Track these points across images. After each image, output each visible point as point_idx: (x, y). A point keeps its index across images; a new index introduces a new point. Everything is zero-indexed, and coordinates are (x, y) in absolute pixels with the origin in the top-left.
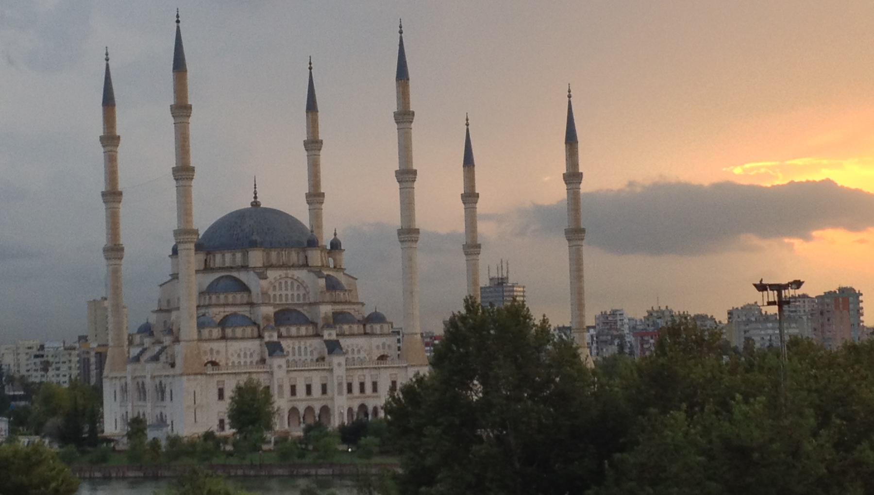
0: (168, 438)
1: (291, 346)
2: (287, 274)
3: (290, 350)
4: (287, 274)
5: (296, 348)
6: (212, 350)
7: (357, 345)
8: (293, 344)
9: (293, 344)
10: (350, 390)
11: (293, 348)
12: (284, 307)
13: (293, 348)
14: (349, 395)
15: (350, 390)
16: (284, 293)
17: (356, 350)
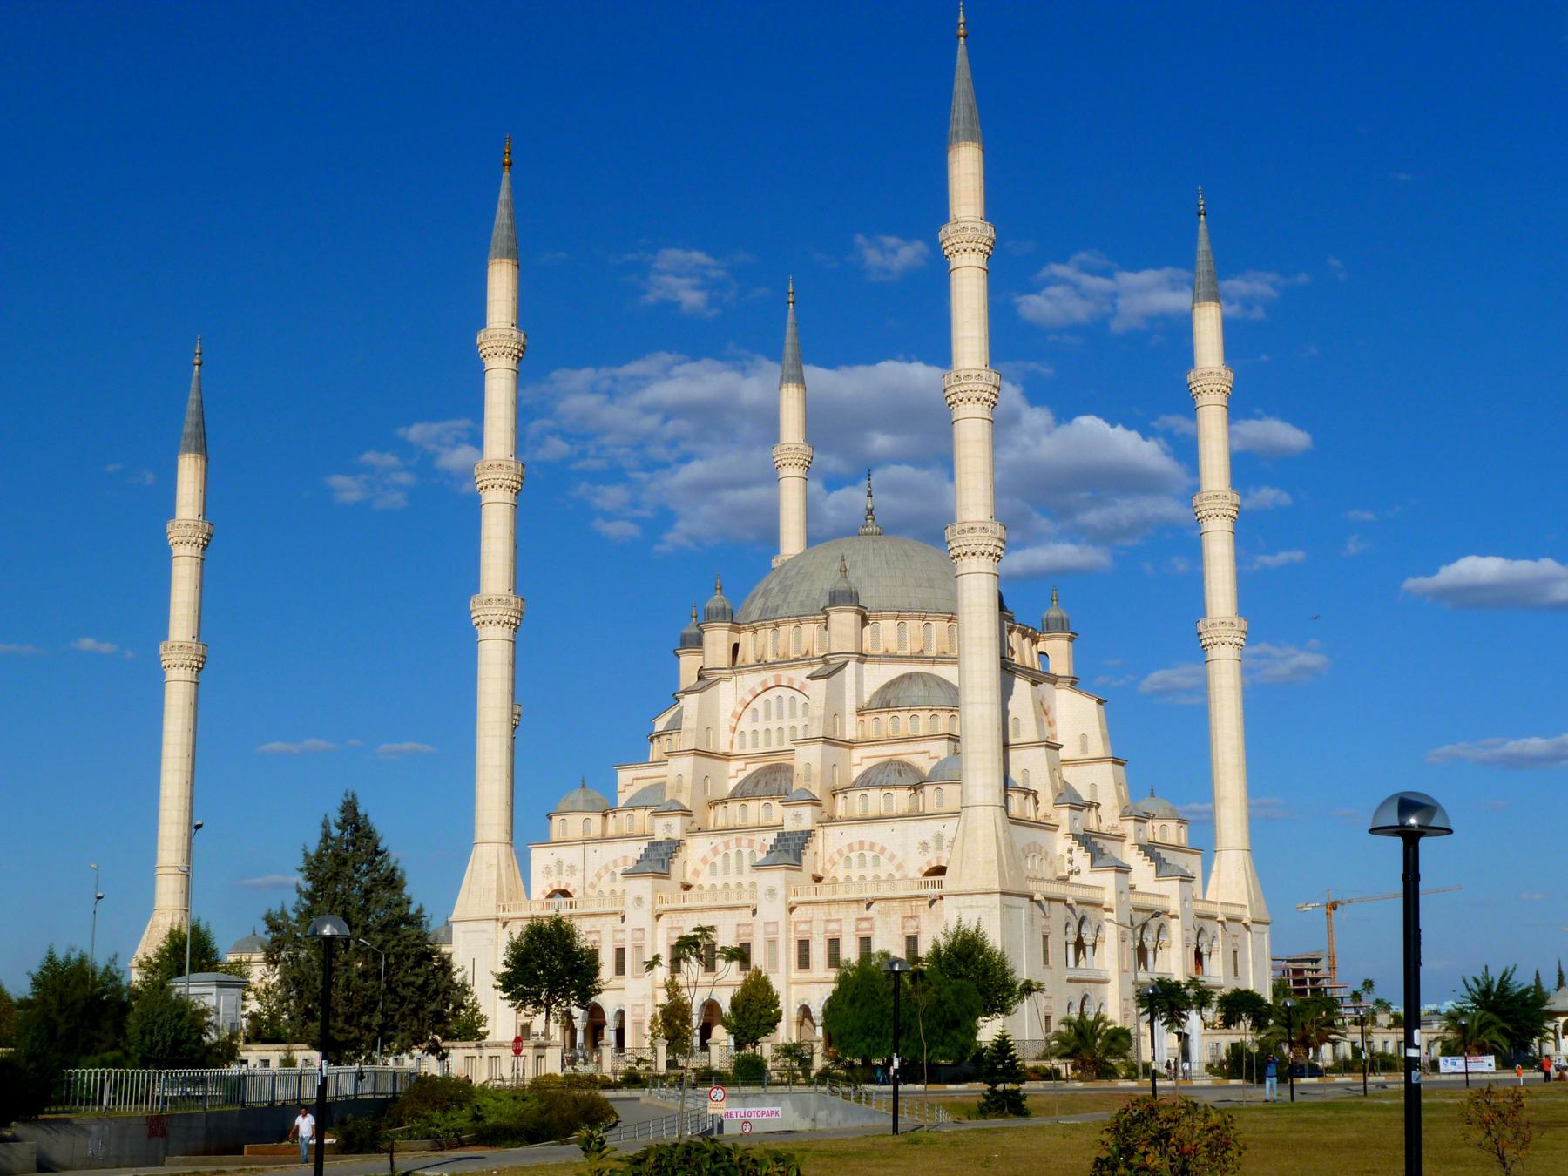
0: (1261, 1081)
1: (721, 849)
2: (778, 677)
3: (719, 860)
4: (778, 677)
5: (732, 852)
6: (559, 863)
7: (872, 846)
8: (727, 845)
9: (727, 845)
10: (804, 962)
11: (726, 855)
12: (773, 760)
13: (726, 855)
14: (804, 975)
15: (804, 962)
16: (773, 725)
17: (869, 855)
